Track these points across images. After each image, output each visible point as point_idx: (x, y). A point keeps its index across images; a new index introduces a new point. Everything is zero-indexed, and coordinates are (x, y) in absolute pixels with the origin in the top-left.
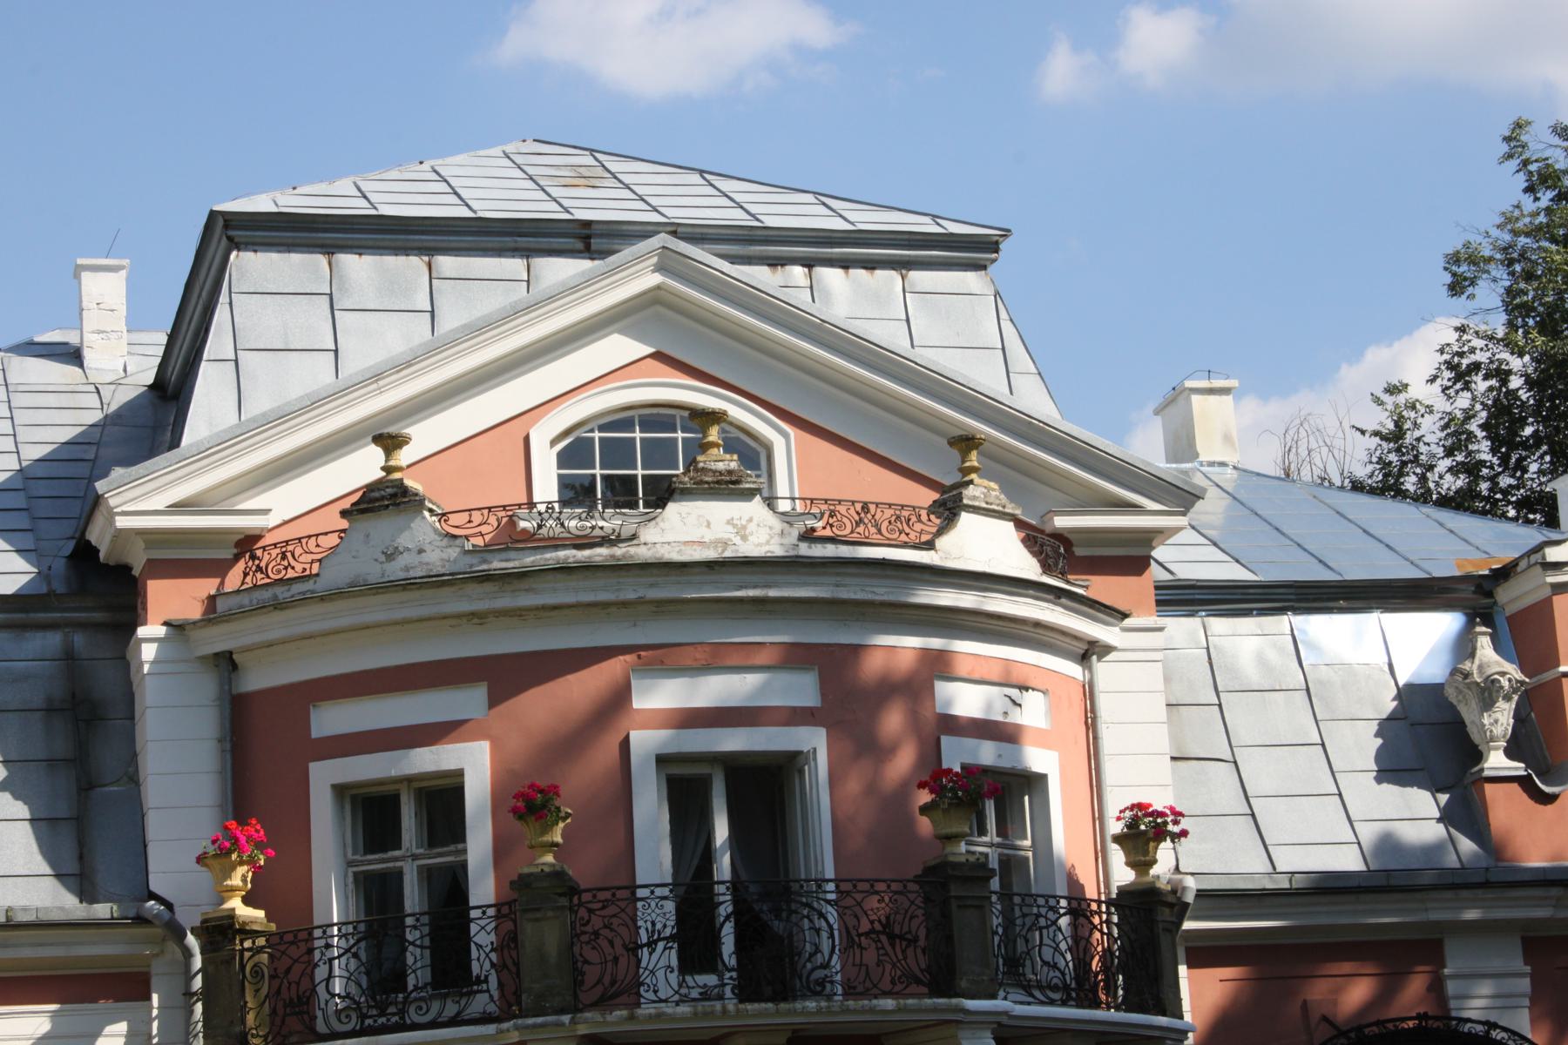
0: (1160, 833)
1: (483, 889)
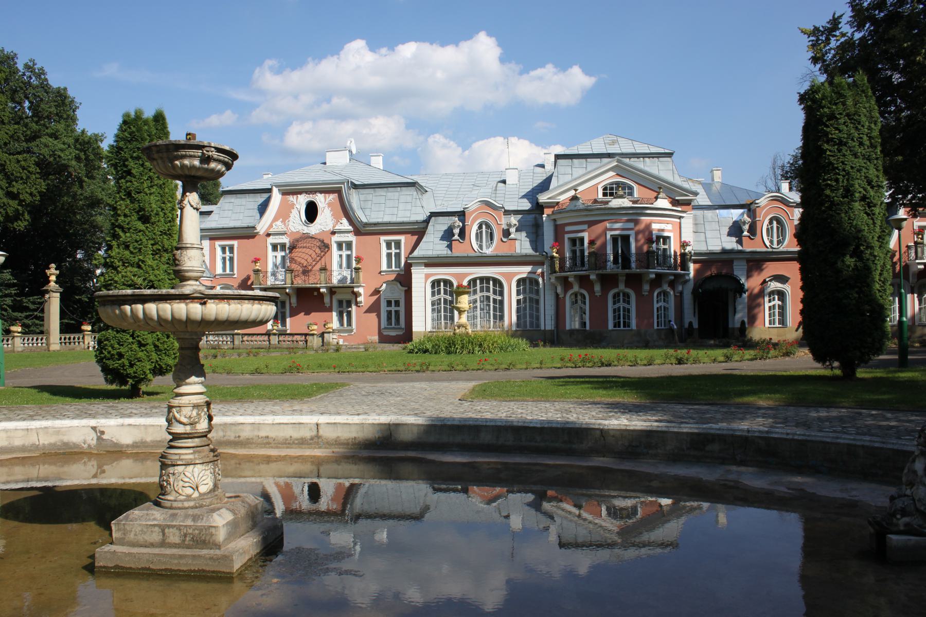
0: (687, 245)
1: (586, 254)
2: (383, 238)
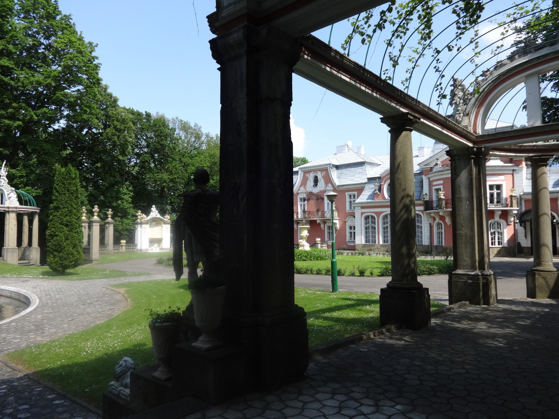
2: (347, 193)
